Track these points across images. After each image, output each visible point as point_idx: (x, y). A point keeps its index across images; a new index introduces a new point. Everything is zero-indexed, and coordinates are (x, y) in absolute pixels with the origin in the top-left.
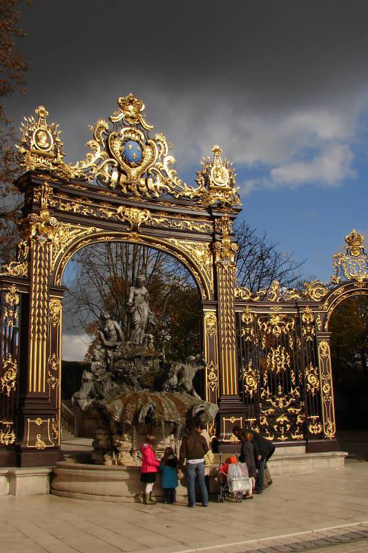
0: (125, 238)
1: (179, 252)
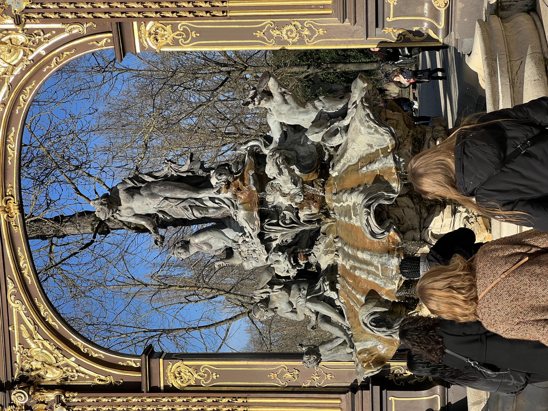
0: (13, 224)
1: (16, 102)
